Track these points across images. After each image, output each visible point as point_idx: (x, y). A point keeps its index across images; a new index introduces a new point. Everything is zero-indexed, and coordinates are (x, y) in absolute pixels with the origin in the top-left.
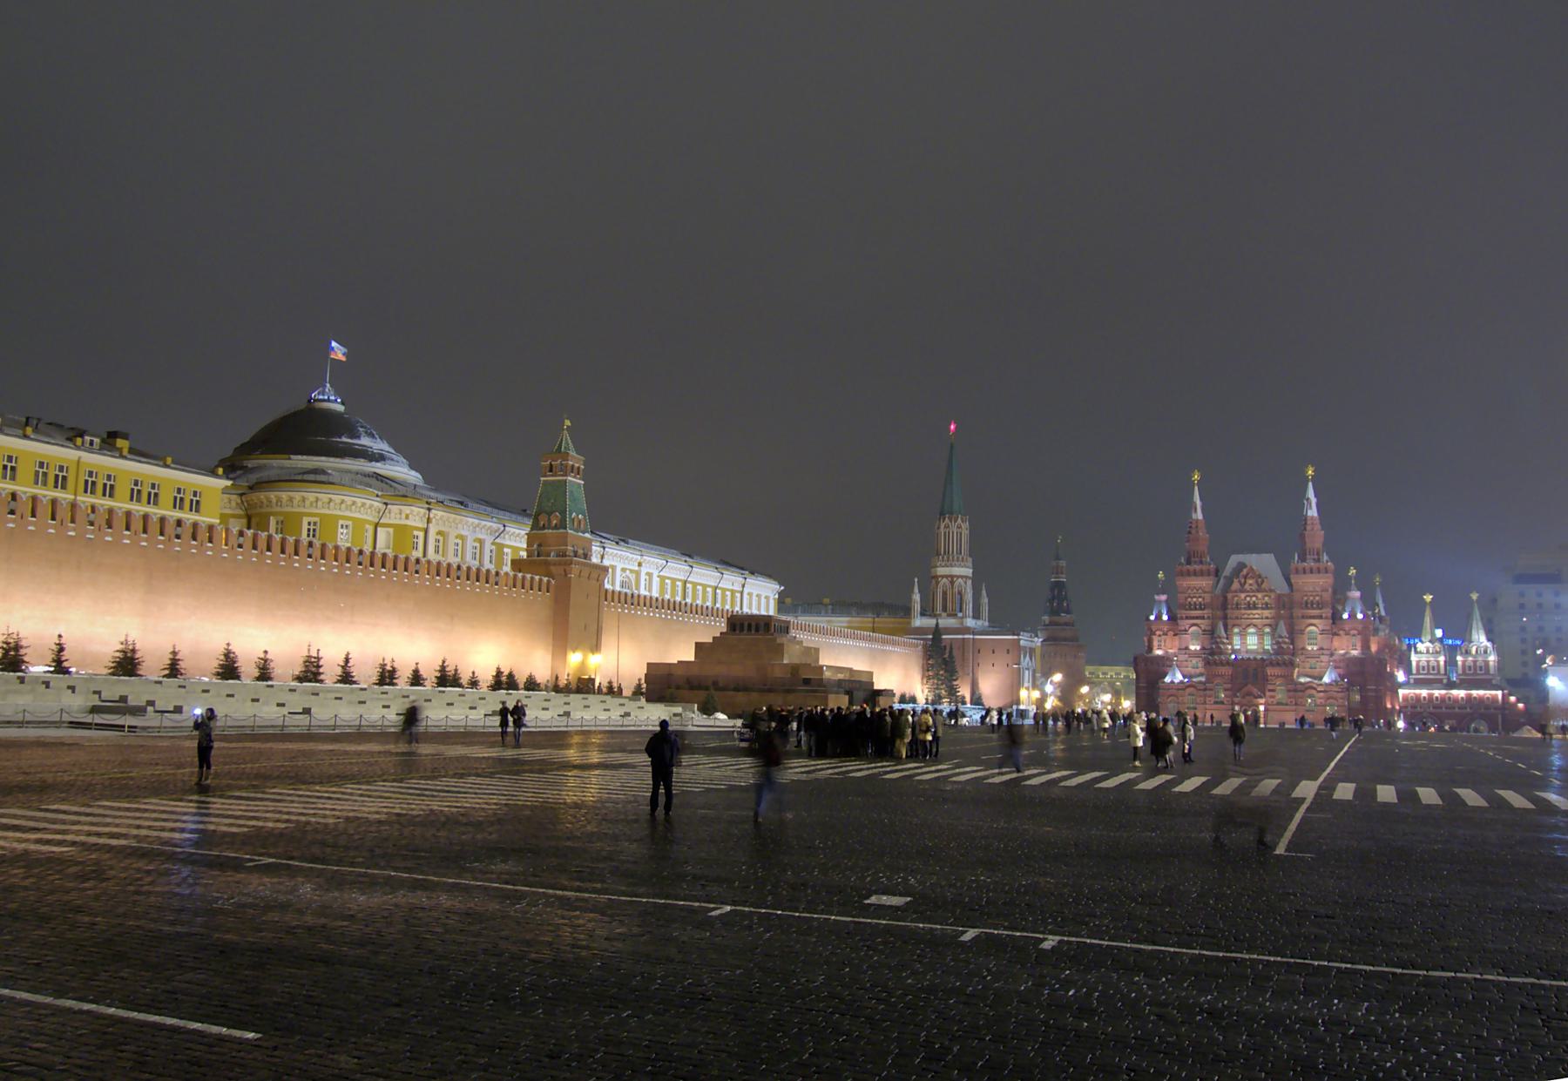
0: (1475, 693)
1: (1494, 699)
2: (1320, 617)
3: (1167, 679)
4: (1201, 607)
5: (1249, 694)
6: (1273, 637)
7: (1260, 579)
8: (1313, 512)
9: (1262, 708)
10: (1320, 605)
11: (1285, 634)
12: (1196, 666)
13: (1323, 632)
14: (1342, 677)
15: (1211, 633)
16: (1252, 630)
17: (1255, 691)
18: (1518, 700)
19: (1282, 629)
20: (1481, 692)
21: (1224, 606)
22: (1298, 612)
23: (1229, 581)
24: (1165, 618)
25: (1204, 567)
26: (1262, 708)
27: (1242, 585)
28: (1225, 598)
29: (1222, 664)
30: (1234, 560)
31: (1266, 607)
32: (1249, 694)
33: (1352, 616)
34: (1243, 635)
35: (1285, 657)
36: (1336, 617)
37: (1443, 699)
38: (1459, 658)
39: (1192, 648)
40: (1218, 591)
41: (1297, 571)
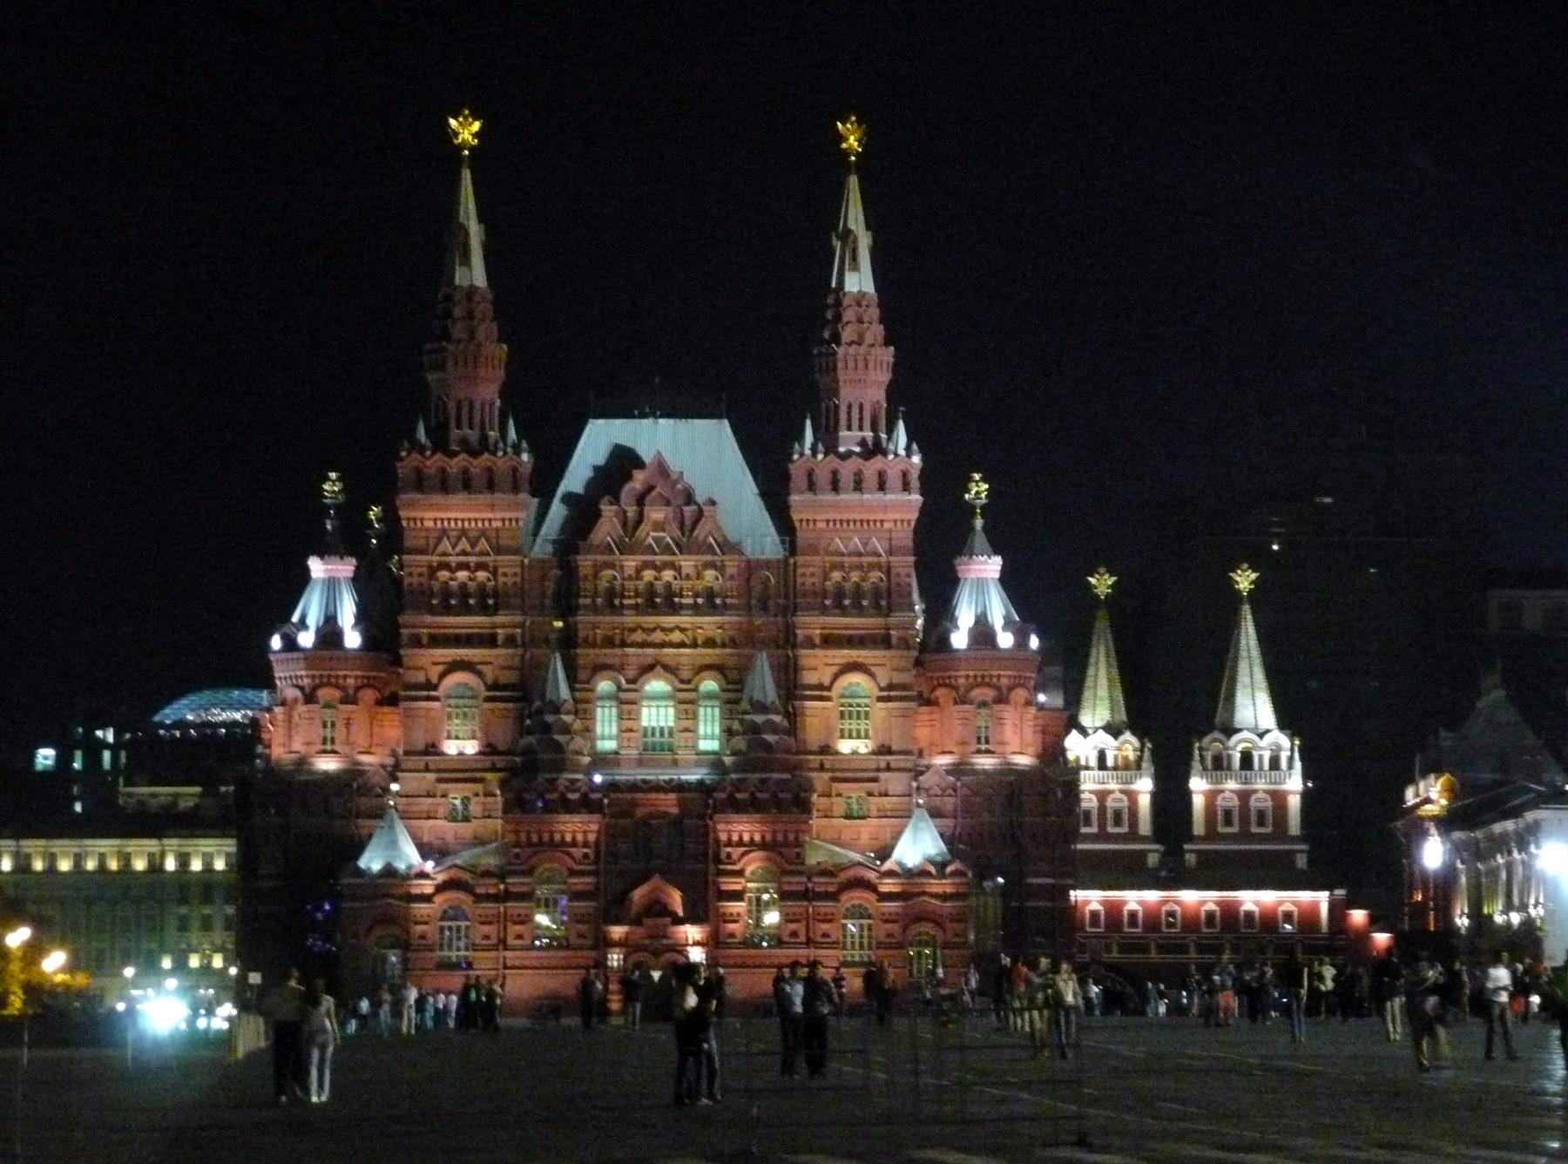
0: (1251, 900)
3: (372, 861)
4: (487, 601)
7: (691, 512)
8: (859, 281)
11: (771, 694)
16: (657, 685)
17: (676, 900)
20: (1268, 897)
21: (566, 603)
22: (811, 624)
24: (353, 640)
25: (501, 462)
27: (631, 526)
28: (569, 572)
29: (569, 807)
30: (597, 440)
31: (710, 603)
34: (627, 703)
35: (773, 773)
37: (1152, 920)
38: (1198, 785)
39: (451, 748)
40: (542, 549)
41: (812, 486)
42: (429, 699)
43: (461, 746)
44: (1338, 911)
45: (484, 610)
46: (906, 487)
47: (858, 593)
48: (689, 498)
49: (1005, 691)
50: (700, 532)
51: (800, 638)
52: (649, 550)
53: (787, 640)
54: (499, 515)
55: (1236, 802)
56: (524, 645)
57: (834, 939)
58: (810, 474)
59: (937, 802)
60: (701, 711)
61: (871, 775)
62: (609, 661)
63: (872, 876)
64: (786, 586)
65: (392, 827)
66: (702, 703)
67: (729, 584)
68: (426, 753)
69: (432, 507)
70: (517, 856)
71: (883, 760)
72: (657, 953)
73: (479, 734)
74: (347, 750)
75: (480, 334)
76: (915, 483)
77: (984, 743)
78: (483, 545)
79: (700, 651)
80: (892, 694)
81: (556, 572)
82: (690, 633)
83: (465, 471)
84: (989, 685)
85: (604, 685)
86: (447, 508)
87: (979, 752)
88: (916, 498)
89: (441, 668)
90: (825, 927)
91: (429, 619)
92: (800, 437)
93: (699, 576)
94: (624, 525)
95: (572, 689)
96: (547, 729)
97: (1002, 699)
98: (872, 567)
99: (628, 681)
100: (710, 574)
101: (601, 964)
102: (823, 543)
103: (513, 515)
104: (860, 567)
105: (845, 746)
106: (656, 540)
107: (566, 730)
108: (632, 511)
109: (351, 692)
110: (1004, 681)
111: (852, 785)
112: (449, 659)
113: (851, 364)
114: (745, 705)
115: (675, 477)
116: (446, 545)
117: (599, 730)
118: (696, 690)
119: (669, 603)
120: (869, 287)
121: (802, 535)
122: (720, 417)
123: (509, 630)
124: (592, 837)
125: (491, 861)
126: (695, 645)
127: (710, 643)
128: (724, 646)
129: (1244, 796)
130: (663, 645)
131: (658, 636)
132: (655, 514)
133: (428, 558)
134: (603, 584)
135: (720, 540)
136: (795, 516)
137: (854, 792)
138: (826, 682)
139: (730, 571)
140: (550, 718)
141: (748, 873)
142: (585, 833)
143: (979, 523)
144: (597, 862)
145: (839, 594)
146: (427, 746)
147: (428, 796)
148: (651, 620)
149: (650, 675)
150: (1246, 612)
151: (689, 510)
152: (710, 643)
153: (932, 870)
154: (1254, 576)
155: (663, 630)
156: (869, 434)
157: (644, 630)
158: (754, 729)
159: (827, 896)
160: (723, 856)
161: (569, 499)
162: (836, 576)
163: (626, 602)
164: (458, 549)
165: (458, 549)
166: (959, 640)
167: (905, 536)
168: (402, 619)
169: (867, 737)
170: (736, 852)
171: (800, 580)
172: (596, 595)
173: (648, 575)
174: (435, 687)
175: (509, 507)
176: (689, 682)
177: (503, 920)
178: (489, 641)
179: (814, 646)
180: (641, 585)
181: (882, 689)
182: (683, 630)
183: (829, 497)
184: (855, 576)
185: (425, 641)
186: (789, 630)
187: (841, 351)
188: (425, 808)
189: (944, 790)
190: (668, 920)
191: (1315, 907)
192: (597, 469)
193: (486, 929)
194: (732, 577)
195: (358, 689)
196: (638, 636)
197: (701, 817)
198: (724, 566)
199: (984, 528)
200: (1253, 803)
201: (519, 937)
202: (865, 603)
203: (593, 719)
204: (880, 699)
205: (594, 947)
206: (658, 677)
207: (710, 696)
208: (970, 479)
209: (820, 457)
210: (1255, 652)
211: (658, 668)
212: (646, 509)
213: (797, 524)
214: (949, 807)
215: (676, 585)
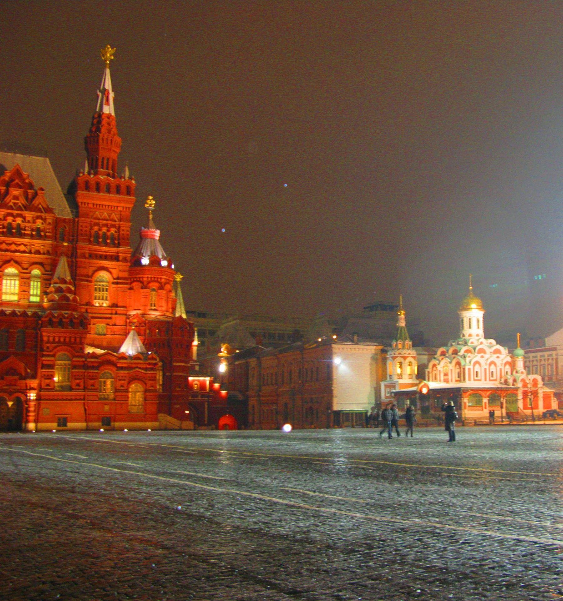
1: (202, 386)
2: (116, 258)
5: (12, 371)
6: (46, 280)
8: (109, 109)
9: (32, 396)
16: (11, 270)
18: (221, 388)
19: (63, 269)
22: (84, 247)
31: (38, 234)
32: (12, 371)
33: (155, 261)
41: (87, 187)
44: (212, 383)
46: (129, 193)
48: (31, 186)
49: (163, 285)
50: (36, 202)
51: (79, 254)
52: (11, 208)
60: (32, 283)
61: (110, 316)
72: (11, 393)
79: (32, 255)
82: (28, 247)
87: (151, 309)
93: (34, 222)
97: (161, 288)
98: (114, 226)
104: (107, 225)
105: (97, 303)
106: (14, 203)
113: (105, 141)
118: (30, 273)
121: (82, 209)
126: (30, 253)
127: (38, 252)
128: (44, 254)
131: (13, 247)
135: (45, 206)
136: (80, 200)
138: (90, 274)
139: (49, 221)
143: (151, 216)
145: (97, 236)
148: (10, 239)
151: (30, 192)
152: (38, 252)
155: (16, 244)
157: (7, 244)
159: (93, 368)
160: (45, 348)
162: (96, 228)
166: (145, 261)
169: (106, 300)
171: (80, 228)
173: (10, 219)
176: (27, 269)
179: (84, 257)
180: (6, 224)
181: (114, 279)
184: (104, 230)
187: (101, 135)
189: (140, 324)
190: (16, 377)
191: (204, 382)
194: (50, 224)
198: (46, 219)
199: (153, 219)
204: (113, 283)
206: (12, 266)
207: (36, 277)
208: (148, 199)
210: (182, 301)
211: (12, 262)
212: (11, 189)
213: (80, 204)
215: (23, 225)
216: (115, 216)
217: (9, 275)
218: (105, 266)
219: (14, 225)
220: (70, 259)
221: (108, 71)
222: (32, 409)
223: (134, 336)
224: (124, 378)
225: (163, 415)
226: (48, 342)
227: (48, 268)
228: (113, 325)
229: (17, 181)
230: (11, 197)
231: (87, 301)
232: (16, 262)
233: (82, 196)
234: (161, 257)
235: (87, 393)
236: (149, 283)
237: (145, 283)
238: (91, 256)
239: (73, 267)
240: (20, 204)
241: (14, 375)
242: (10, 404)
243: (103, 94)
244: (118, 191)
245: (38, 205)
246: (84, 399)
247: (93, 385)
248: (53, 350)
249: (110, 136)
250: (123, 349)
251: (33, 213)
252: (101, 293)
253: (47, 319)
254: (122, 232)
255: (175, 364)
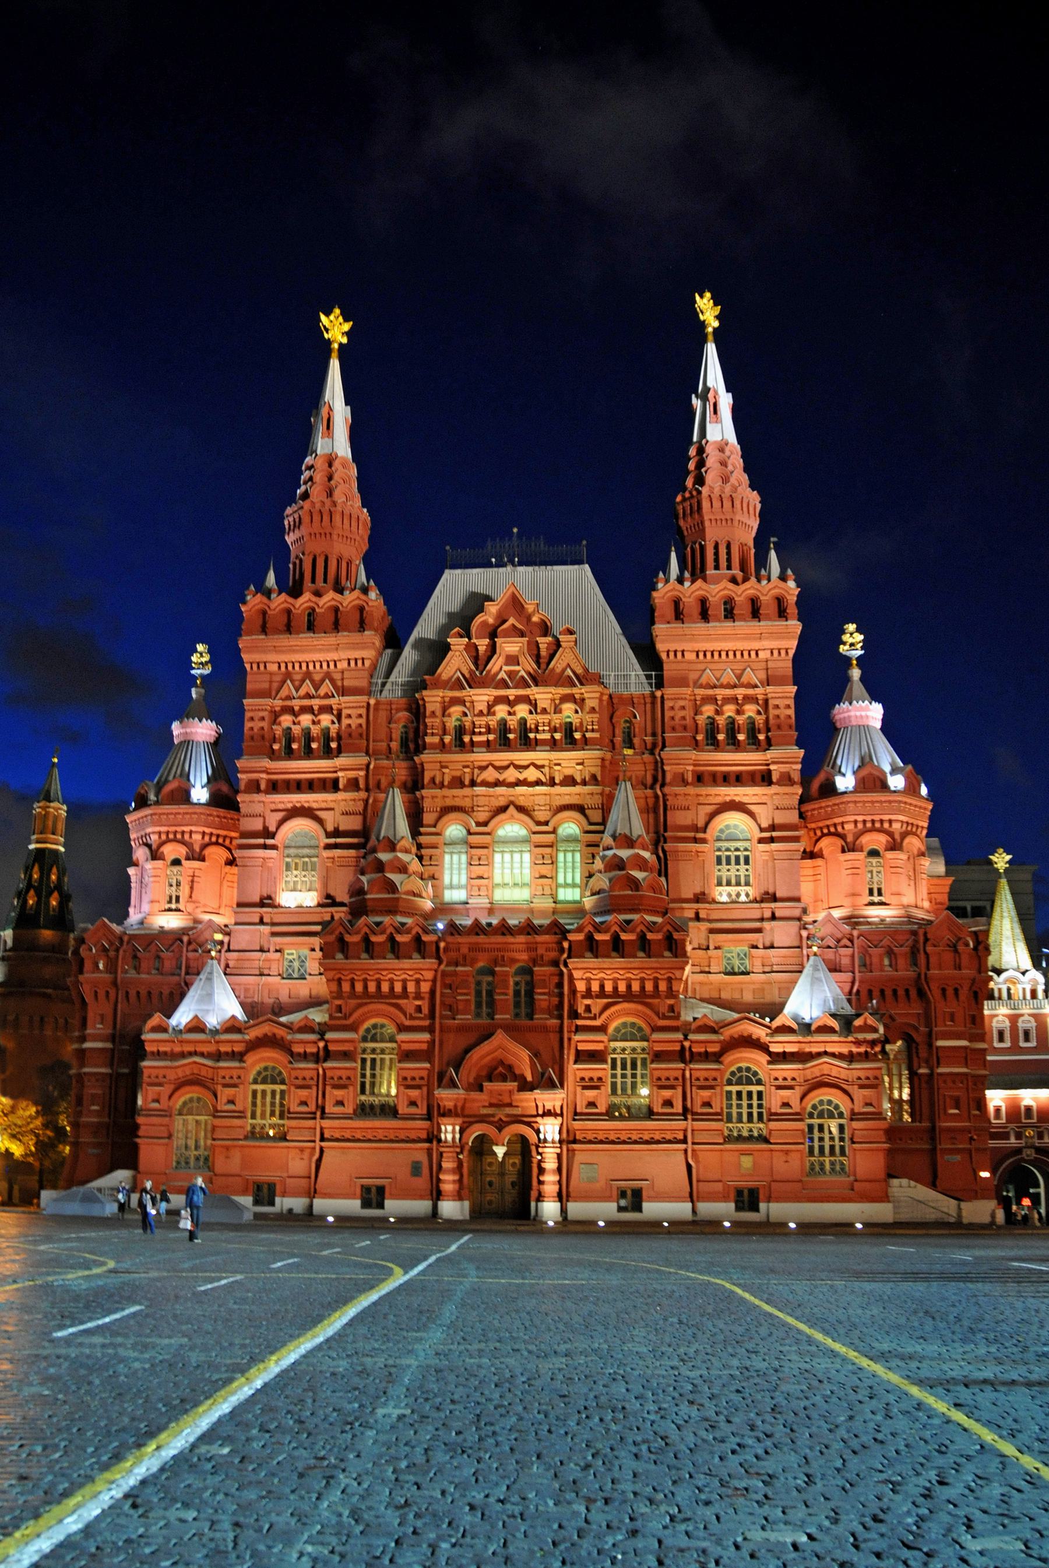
2: (765, 778)
4: (329, 746)
8: (720, 430)
9: (550, 1129)
10: (757, 737)
11: (638, 828)
12: (298, 970)
13: (771, 834)
14: (857, 998)
15: (362, 840)
16: (511, 828)
17: (523, 1061)
19: (628, 814)
21: (413, 743)
22: (681, 759)
23: (439, 650)
24: (200, 794)
25: (349, 599)
26: (550, 1129)
28: (417, 711)
30: (454, 586)
31: (569, 738)
34: (479, 846)
35: (643, 915)
36: (815, 785)
41: (679, 615)
42: (265, 847)
43: (298, 896)
45: (328, 753)
46: (782, 613)
47: (732, 729)
48: (545, 629)
49: (897, 837)
50: (558, 664)
53: (655, 780)
54: (344, 654)
55: (1007, 1023)
56: (367, 790)
57: (716, 1109)
58: (677, 603)
59: (830, 954)
60: (561, 856)
61: (757, 925)
62: (458, 802)
63: (760, 1033)
64: (654, 720)
65: (209, 979)
66: (562, 847)
67: (588, 718)
68: (261, 904)
69: (276, 649)
70: (339, 1009)
71: (767, 908)
72: (500, 1126)
73: (317, 885)
74: (190, 907)
75: (339, 496)
76: (792, 610)
77: (876, 895)
78: (327, 687)
79: (558, 789)
80: (774, 834)
81: (403, 715)
82: (546, 770)
83: (312, 613)
84: (881, 830)
85: (454, 830)
86: (292, 650)
88: (795, 626)
89: (280, 815)
90: (706, 1094)
91: (266, 763)
92: (665, 567)
93: (557, 710)
94: (476, 659)
95: (415, 833)
96: (380, 867)
97: (895, 846)
98: (748, 699)
99: (478, 824)
100: (568, 708)
101: (433, 1137)
102: (693, 676)
103: (358, 654)
104: (734, 700)
105: (722, 894)
106: (510, 674)
107: (403, 869)
108: (483, 644)
109: (197, 848)
110: (896, 826)
111: (730, 936)
112: (289, 806)
113: (717, 504)
114: (607, 839)
115: (530, 608)
116: (289, 688)
117: (447, 880)
118: (554, 831)
119: (526, 740)
120: (731, 437)
121: (670, 669)
122: (579, 562)
123: (352, 774)
124: (425, 987)
125: (318, 1016)
126: (552, 783)
127: (569, 781)
128: (584, 783)
129: (1014, 1019)
130: (519, 783)
131: (511, 775)
132: (510, 646)
133: (269, 701)
134: (452, 723)
135: (580, 671)
136: (661, 647)
137: (734, 948)
138: (701, 823)
139: (590, 703)
140: (384, 856)
141: (611, 1029)
142: (418, 982)
143: (856, 673)
144: (432, 1015)
146: (262, 899)
147: (262, 950)
148: (502, 757)
149: (502, 816)
150: (1004, 883)
151: (544, 642)
152: (569, 781)
153: (834, 1024)
154: (1009, 857)
155: (517, 767)
156: (736, 572)
157: (496, 768)
158: (617, 865)
159: (706, 1057)
160: (581, 1010)
161: (419, 644)
162: (708, 710)
163: (476, 739)
164: (302, 691)
165: (302, 691)
166: (845, 782)
167: (785, 665)
168: (240, 763)
169: (747, 884)
170: (597, 1005)
171: (668, 714)
172: (445, 732)
173: (501, 711)
174: (273, 836)
175: (355, 646)
176: (546, 823)
177: (323, 1082)
178: (333, 786)
179: (684, 782)
181: (762, 830)
182: (538, 767)
183: (701, 627)
184: (729, 710)
185: (263, 786)
186: (659, 766)
187: (705, 490)
188: (256, 964)
189: (838, 941)
192: (450, 615)
193: (303, 1093)
194: (593, 710)
195: (204, 847)
196: (490, 775)
197: (555, 963)
198: (583, 700)
199: (862, 679)
200: (1020, 1024)
201: (340, 1103)
202: (741, 737)
203: (440, 865)
204: (761, 841)
205: (429, 1117)
207: (570, 839)
208: (843, 632)
209: (687, 584)
211: (512, 810)
213: (664, 656)
214: (845, 961)
216: (750, 676)
217: (506, 841)
218: (737, 799)
219: (513, 722)
220: (649, 791)
221: (711, 350)
222: (550, 1164)
223: (816, 969)
224: (789, 1083)
225: (904, 1182)
226: (588, 994)
227: (596, 816)
228: (765, 948)
229: (512, 621)
230: (501, 660)
231: (698, 890)
232: (521, 809)
233: (667, 637)
234: (887, 768)
235: (689, 1124)
236: (858, 835)
237: (850, 838)
238: (700, 779)
239: (657, 812)
240: (523, 673)
241: (504, 1079)
242: (500, 1151)
243: (704, 398)
244: (756, 613)
245: (564, 670)
246: (684, 1141)
247: (708, 1104)
248: (601, 1014)
249: (728, 488)
250: (789, 1009)
251: (552, 689)
252: (733, 867)
253: (580, 937)
254: (772, 712)
255: (940, 1043)
